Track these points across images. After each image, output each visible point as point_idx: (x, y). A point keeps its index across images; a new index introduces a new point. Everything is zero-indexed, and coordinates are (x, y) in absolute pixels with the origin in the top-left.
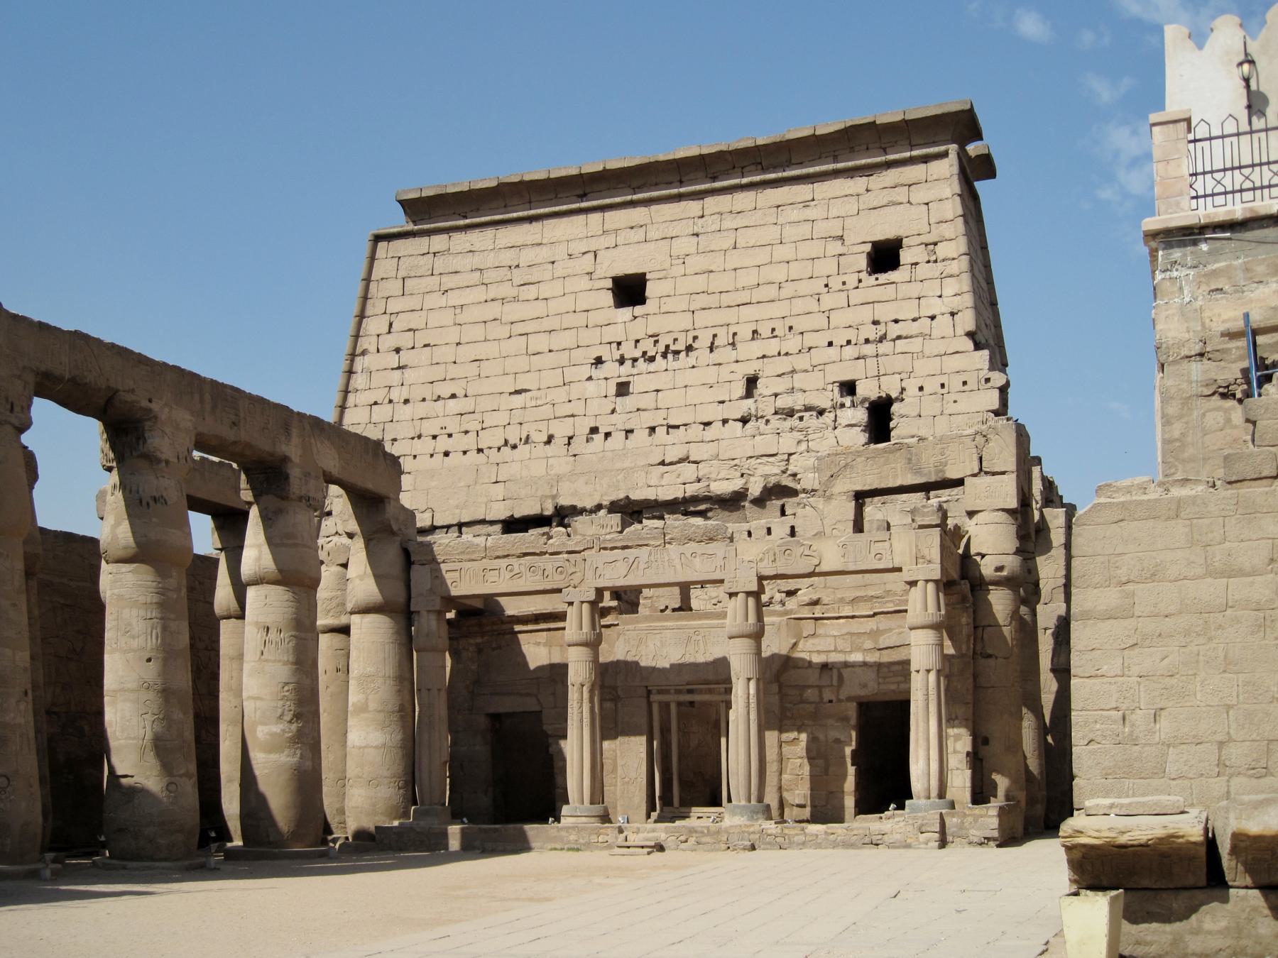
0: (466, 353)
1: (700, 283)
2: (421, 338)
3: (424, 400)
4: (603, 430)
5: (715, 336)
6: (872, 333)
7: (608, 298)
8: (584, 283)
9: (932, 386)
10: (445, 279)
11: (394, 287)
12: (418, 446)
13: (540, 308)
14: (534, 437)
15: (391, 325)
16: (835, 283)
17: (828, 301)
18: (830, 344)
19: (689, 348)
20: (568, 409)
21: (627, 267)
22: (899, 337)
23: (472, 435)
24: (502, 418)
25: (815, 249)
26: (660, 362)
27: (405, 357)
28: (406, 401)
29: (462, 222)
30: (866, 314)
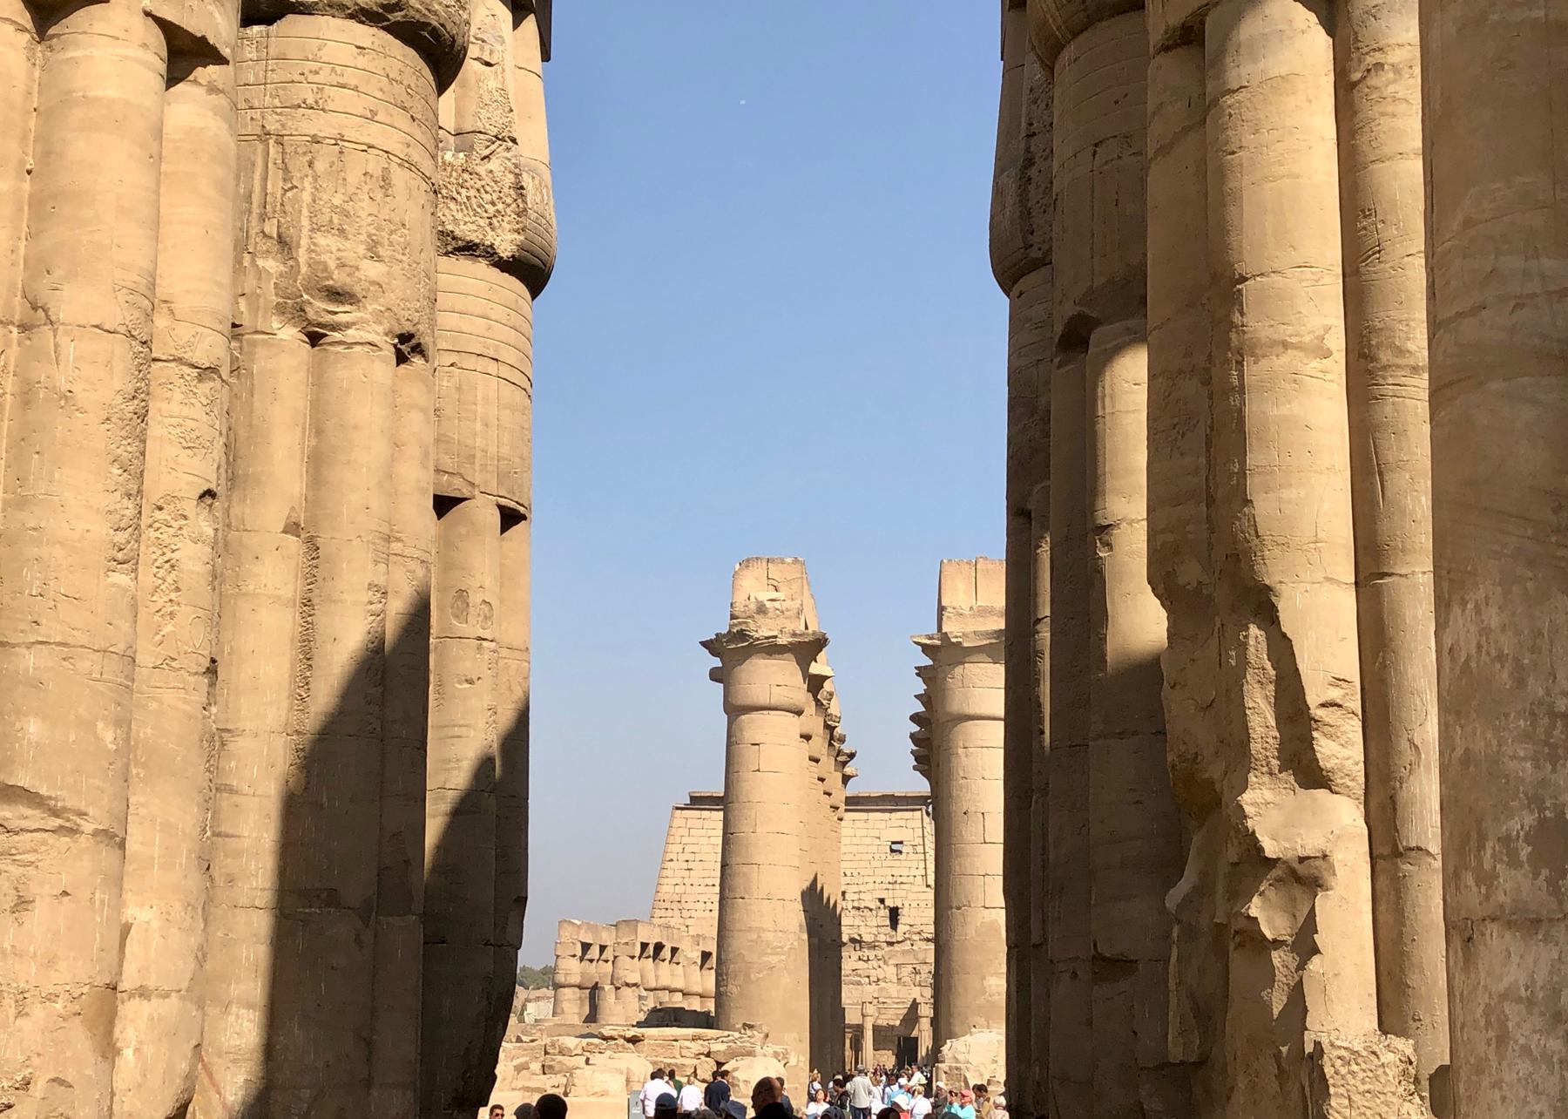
2: (698, 857)
9: (914, 904)
11: (685, 832)
17: (876, 864)
27: (691, 865)
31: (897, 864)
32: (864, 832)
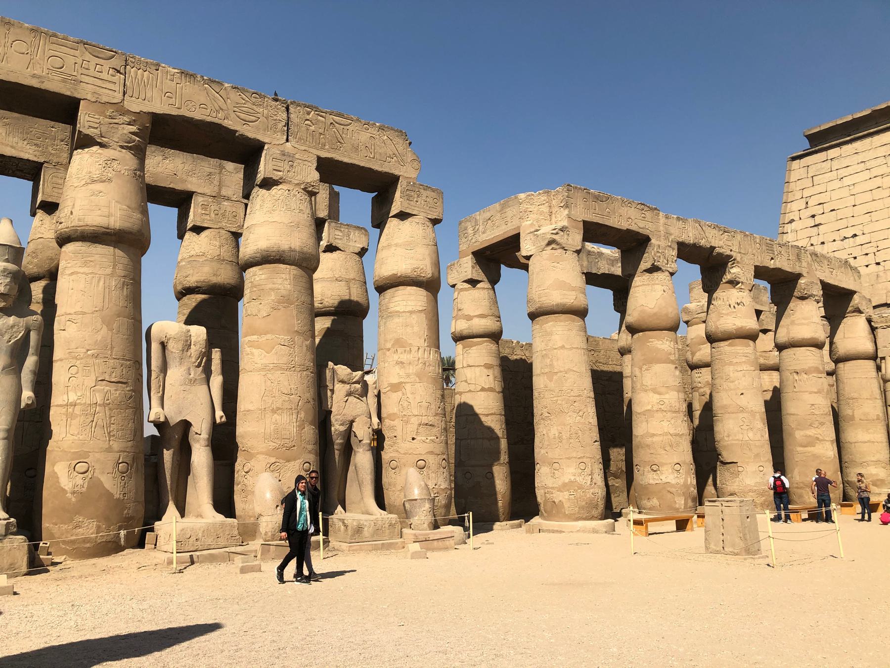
23: (871, 256)
27: (818, 220)
29: (848, 138)
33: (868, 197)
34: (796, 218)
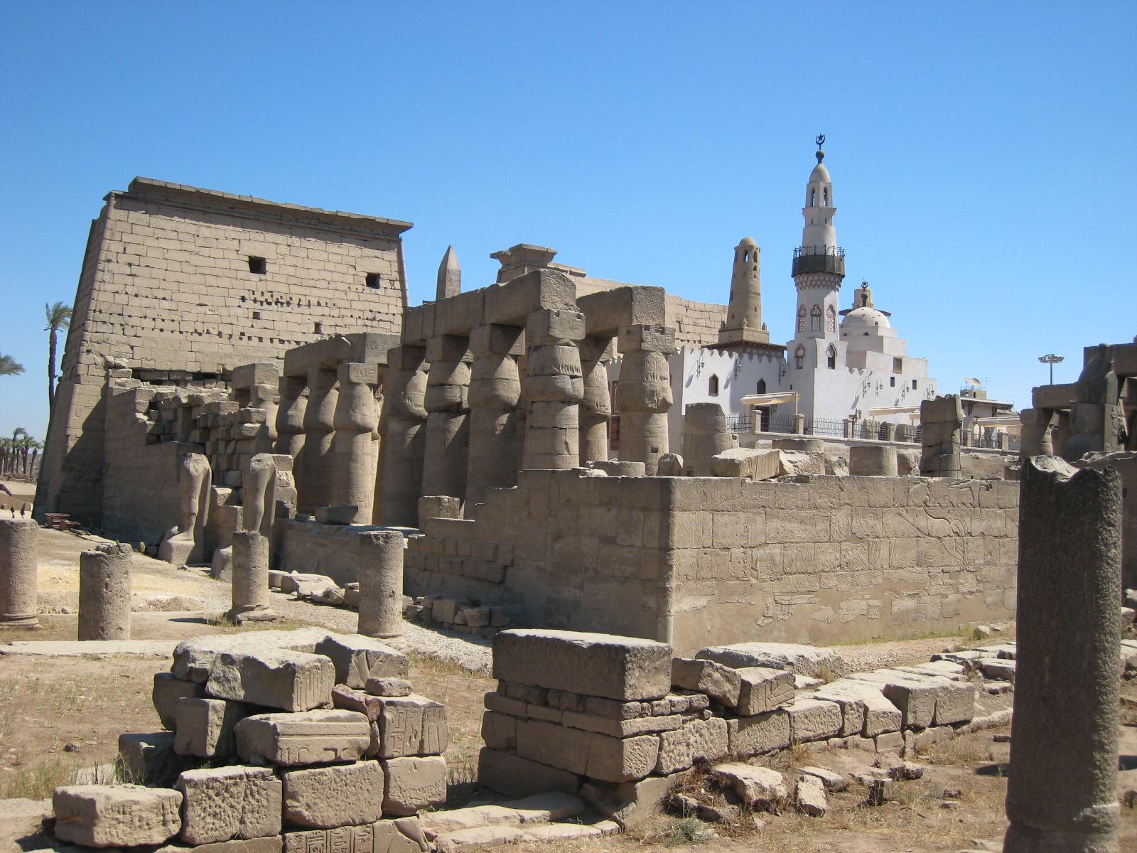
0: (172, 276)
1: (291, 271)
2: (144, 262)
3: (147, 297)
4: (247, 335)
5: (300, 300)
6: (370, 316)
7: (247, 267)
8: (234, 255)
10: (156, 231)
11: (127, 228)
12: (145, 323)
13: (211, 262)
14: (211, 330)
15: (125, 249)
16: (353, 288)
17: (352, 296)
18: (352, 316)
19: (288, 304)
20: (228, 320)
21: (257, 253)
22: (381, 320)
23: (176, 324)
24: (193, 317)
25: (344, 269)
26: (274, 307)
27: (135, 270)
28: (136, 296)
30: (367, 306)
31: (375, 298)
32: (339, 258)
33: (177, 267)
34: (114, 260)
